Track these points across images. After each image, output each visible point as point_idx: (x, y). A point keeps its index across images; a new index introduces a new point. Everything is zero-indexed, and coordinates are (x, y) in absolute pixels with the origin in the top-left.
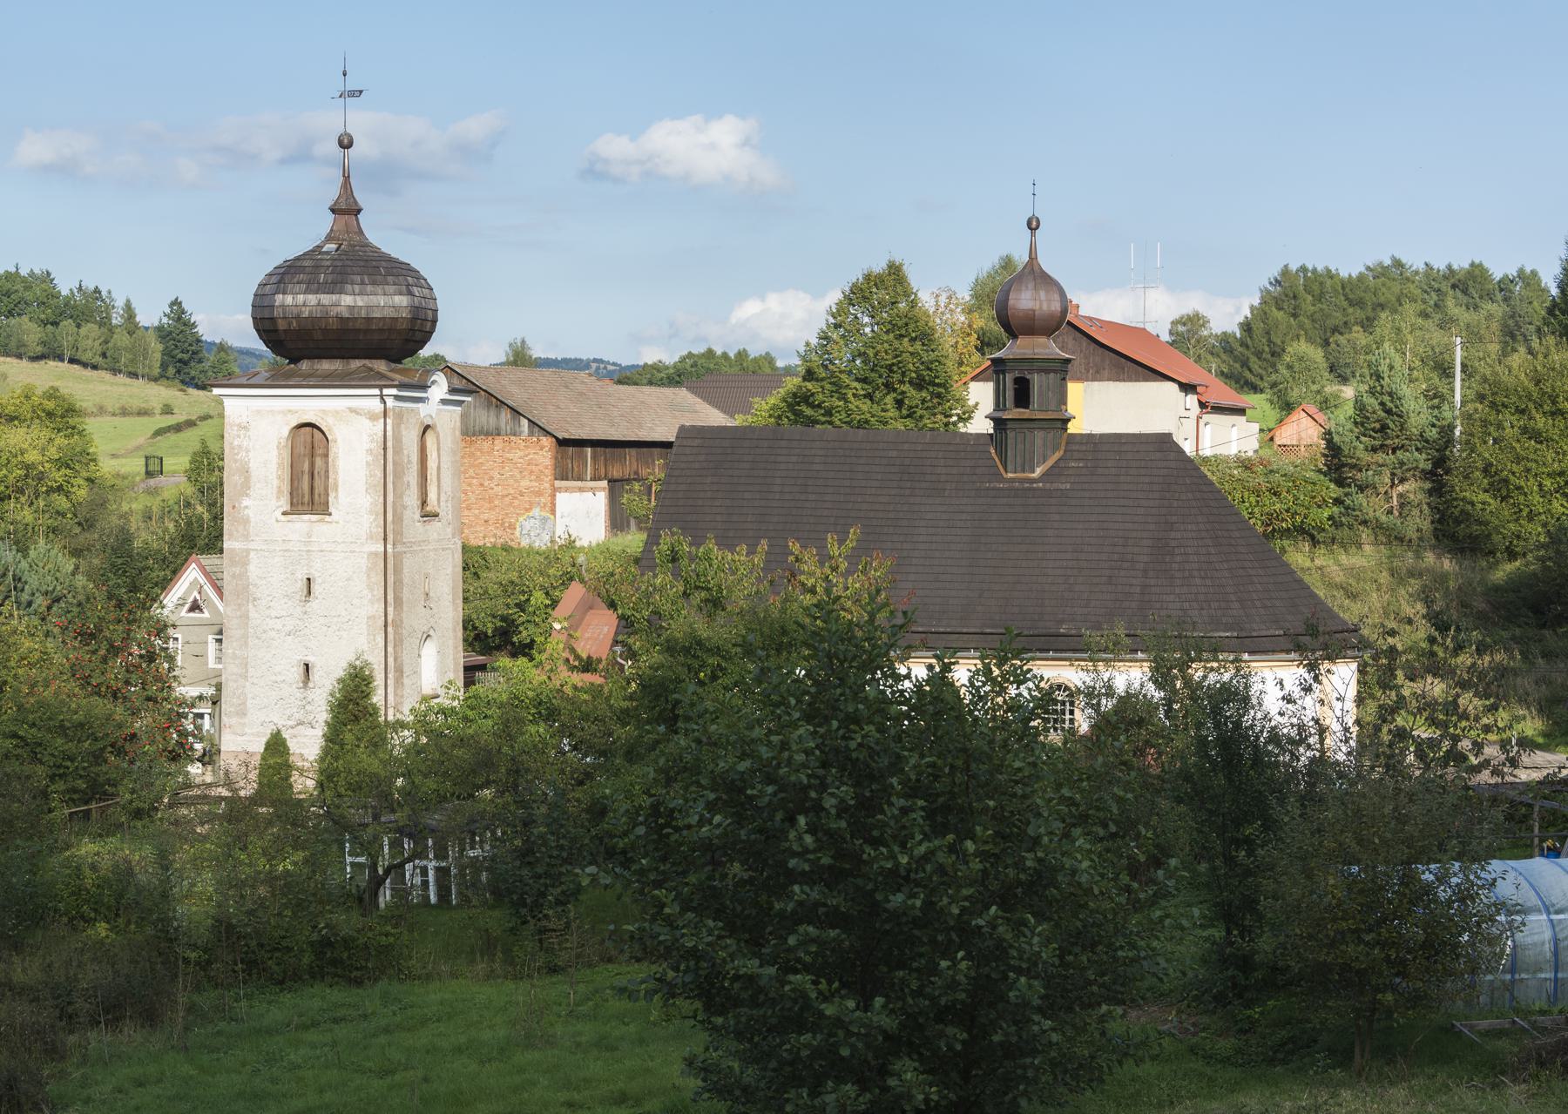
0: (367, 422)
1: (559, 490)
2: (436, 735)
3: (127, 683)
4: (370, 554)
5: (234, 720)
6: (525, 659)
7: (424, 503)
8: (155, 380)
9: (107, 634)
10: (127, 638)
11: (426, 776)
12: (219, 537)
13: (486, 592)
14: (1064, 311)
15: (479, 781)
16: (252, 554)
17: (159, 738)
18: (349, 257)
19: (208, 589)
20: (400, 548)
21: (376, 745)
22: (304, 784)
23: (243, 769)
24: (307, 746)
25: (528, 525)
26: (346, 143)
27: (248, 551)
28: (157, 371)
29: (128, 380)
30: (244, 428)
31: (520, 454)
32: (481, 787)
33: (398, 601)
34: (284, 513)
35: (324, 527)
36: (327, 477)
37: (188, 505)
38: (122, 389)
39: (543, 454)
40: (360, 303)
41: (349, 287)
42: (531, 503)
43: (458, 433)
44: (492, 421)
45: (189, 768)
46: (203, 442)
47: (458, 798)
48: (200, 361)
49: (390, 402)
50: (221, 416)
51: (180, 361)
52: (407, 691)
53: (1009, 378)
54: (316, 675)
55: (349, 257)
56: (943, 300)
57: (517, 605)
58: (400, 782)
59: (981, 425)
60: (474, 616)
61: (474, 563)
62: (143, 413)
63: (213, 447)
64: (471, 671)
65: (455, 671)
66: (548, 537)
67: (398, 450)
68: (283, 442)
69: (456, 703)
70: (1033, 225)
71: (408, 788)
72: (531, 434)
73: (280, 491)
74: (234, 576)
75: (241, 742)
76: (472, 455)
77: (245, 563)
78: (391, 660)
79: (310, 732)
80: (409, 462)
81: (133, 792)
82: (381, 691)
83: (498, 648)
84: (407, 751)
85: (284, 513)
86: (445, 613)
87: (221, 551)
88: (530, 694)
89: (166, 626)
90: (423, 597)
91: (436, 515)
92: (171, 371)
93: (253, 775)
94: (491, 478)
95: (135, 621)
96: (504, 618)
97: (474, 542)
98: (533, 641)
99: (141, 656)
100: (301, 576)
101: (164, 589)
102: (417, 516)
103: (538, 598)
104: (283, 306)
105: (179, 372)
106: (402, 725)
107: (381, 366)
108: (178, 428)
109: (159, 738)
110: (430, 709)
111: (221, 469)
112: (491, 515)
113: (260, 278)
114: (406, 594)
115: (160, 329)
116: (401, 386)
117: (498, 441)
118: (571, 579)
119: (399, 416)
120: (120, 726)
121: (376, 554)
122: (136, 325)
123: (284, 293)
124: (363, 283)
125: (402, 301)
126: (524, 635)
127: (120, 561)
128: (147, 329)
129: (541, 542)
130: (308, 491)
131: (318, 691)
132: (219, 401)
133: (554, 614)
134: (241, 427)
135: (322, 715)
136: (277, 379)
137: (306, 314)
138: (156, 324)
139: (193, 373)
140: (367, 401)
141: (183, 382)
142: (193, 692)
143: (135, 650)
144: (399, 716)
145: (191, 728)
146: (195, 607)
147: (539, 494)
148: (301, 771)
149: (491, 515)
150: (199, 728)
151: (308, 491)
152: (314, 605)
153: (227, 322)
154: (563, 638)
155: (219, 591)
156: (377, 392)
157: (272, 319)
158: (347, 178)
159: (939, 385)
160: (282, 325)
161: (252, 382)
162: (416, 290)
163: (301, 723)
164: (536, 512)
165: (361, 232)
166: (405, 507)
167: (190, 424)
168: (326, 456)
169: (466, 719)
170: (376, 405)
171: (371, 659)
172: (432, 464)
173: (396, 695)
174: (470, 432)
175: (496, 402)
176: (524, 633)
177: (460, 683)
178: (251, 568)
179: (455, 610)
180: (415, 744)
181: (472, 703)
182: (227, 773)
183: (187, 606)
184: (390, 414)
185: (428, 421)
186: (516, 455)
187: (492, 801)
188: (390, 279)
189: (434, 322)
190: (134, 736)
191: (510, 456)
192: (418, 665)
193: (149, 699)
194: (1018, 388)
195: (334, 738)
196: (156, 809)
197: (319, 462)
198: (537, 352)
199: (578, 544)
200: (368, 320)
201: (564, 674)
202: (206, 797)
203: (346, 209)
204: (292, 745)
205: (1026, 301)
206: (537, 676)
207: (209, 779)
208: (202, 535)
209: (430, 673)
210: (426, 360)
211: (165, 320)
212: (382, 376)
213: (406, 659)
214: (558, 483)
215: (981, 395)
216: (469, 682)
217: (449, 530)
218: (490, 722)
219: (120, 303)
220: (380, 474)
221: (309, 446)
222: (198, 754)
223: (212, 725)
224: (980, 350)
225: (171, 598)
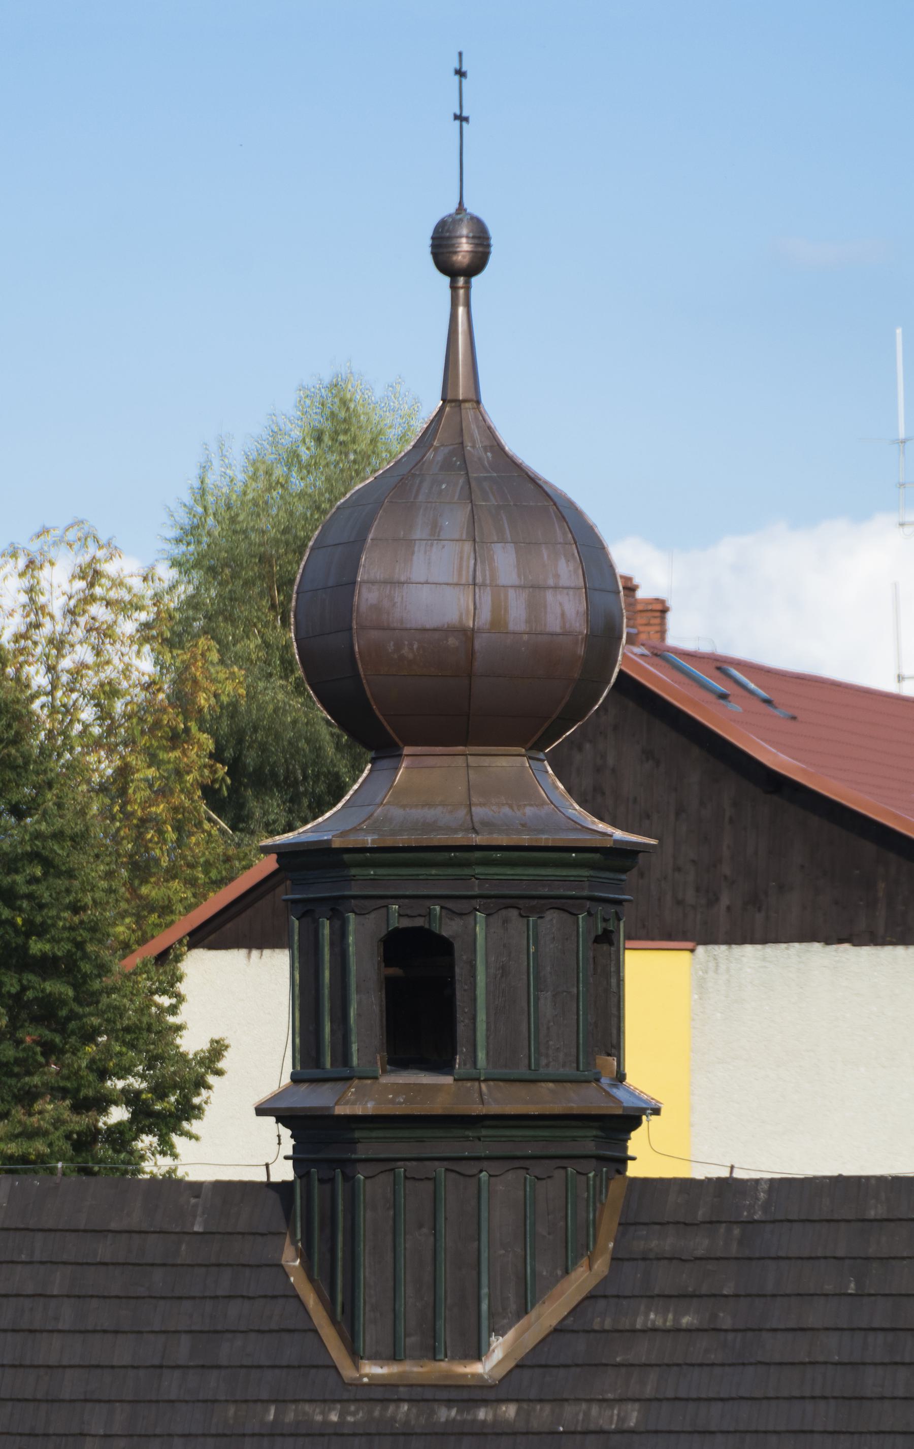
14: (604, 637)
53: (361, 936)
56: (59, 582)
59: (233, 1142)
70: (460, 254)
159: (47, 966)
194: (400, 980)
205: (435, 586)
215: (238, 1009)
224: (228, 803)
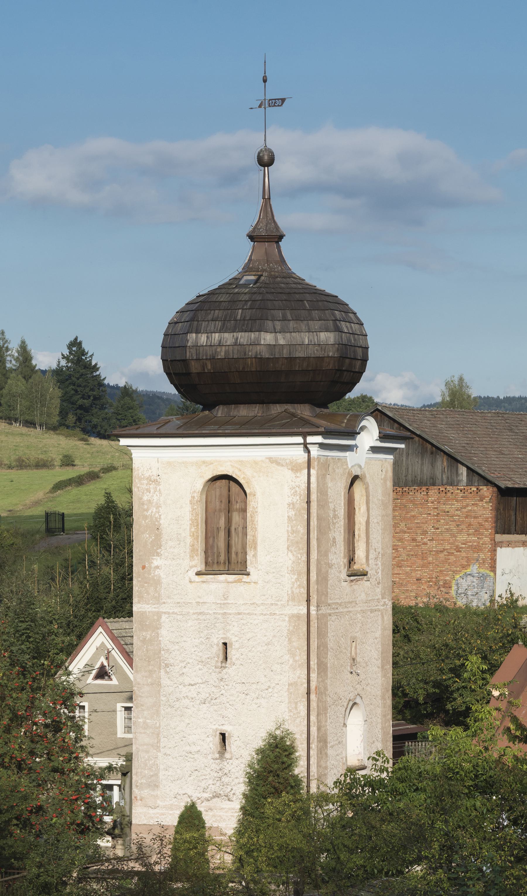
0: (288, 474)
1: (501, 544)
2: (363, 809)
3: (32, 753)
4: (292, 616)
5: (145, 793)
6: (459, 730)
7: (351, 561)
8: (54, 429)
9: (10, 702)
10: (32, 706)
11: (351, 851)
12: (128, 598)
13: (417, 656)
15: (409, 857)
16: (164, 617)
17: (66, 810)
18: (269, 289)
19: (116, 655)
20: (324, 610)
21: (299, 819)
22: (221, 859)
23: (158, 843)
24: (224, 818)
25: (464, 584)
26: (266, 160)
27: (159, 615)
28: (55, 419)
29: (25, 430)
30: (155, 481)
31: (457, 505)
32: (412, 863)
33: (322, 667)
34: (198, 574)
35: (241, 588)
36: (245, 534)
37: (93, 564)
38: (18, 439)
39: (482, 505)
40: (282, 342)
41: (270, 323)
42: (468, 560)
43: (390, 484)
44: (427, 469)
45: (99, 842)
46: (108, 496)
47: (387, 874)
48: (102, 408)
49: (315, 451)
50: (129, 467)
51: (81, 407)
52: (331, 762)
54: (232, 744)
55: (269, 289)
57: (452, 670)
58: (323, 857)
60: (404, 682)
61: (406, 625)
62: (42, 465)
63: (120, 501)
64: (399, 740)
65: (384, 741)
66: (487, 597)
67: (323, 504)
68: (197, 496)
69: (384, 775)
71: (333, 863)
72: (470, 483)
73: (193, 550)
74: (144, 641)
75: (153, 813)
76: (404, 507)
77: (156, 627)
78: (314, 730)
79: (226, 805)
80: (335, 516)
81: (40, 865)
82: (303, 763)
83: (430, 716)
84: (332, 826)
85: (198, 574)
86: (375, 679)
87: (130, 614)
88: (467, 766)
89: (72, 695)
90: (349, 662)
91: (365, 574)
92: (71, 418)
93: (167, 850)
94: (425, 533)
95: (39, 688)
96: (437, 684)
97: (405, 602)
98: (468, 709)
99: (46, 726)
100: (217, 640)
101: (69, 654)
102: (343, 575)
103: (474, 662)
104: (196, 346)
105: (79, 419)
106: (324, 798)
107: (304, 411)
108: (79, 481)
109: (66, 810)
110: (355, 780)
111: (129, 526)
112: (425, 574)
113: (170, 314)
114: (331, 660)
115: (58, 372)
116: (326, 434)
117: (433, 491)
118: (513, 642)
120: (25, 798)
121: (298, 616)
122: (33, 369)
123: (197, 332)
124: (284, 319)
125: (327, 337)
126: (458, 702)
127: (24, 625)
128: (44, 372)
129: (480, 601)
130: (224, 550)
131: (236, 762)
132: (126, 452)
133: (493, 680)
134: (150, 480)
135: (239, 787)
136: (193, 426)
137: (222, 355)
138: (54, 366)
139: (95, 421)
140: (288, 449)
141: (85, 431)
142: (102, 762)
143: (40, 719)
144: (323, 788)
145: (99, 800)
146: (102, 674)
147: (478, 549)
148: (219, 846)
149: (425, 574)
150: (108, 800)
151: (224, 550)
152: (231, 670)
153: (135, 363)
154: (502, 705)
155: (128, 656)
156: (299, 439)
157: (185, 362)
158: (267, 200)
160: (195, 368)
161: (162, 431)
162: (344, 326)
163: (217, 796)
164: (474, 569)
165: (283, 261)
166: (330, 566)
167: (93, 476)
169: (394, 792)
170: (299, 454)
171: (292, 728)
172: (360, 518)
173: (319, 766)
174: (402, 481)
175: (428, 448)
176: (459, 700)
177: (389, 754)
178: (163, 632)
179: (384, 676)
180: (341, 818)
181: (402, 775)
182: (140, 847)
183: (94, 672)
184: (314, 464)
185: (357, 472)
186: (453, 507)
187: (423, 877)
188: (315, 314)
189: (364, 360)
190: (40, 808)
191: (447, 508)
192: (344, 735)
193: (55, 770)
195: (253, 808)
196: (65, 884)
197: (236, 518)
198: (476, 390)
199: (520, 603)
200: (291, 360)
201: (502, 742)
202: (117, 871)
203: (267, 236)
204: (209, 819)
206: (474, 746)
207: (120, 852)
208: (111, 597)
209: (358, 739)
210: (352, 402)
211: (63, 363)
212: (305, 422)
213: (330, 728)
214: (499, 537)
216: (398, 753)
217: (379, 590)
218: (423, 796)
219: (14, 346)
220: (303, 530)
221: (225, 500)
222: (107, 827)
223: (122, 797)
225: (77, 664)
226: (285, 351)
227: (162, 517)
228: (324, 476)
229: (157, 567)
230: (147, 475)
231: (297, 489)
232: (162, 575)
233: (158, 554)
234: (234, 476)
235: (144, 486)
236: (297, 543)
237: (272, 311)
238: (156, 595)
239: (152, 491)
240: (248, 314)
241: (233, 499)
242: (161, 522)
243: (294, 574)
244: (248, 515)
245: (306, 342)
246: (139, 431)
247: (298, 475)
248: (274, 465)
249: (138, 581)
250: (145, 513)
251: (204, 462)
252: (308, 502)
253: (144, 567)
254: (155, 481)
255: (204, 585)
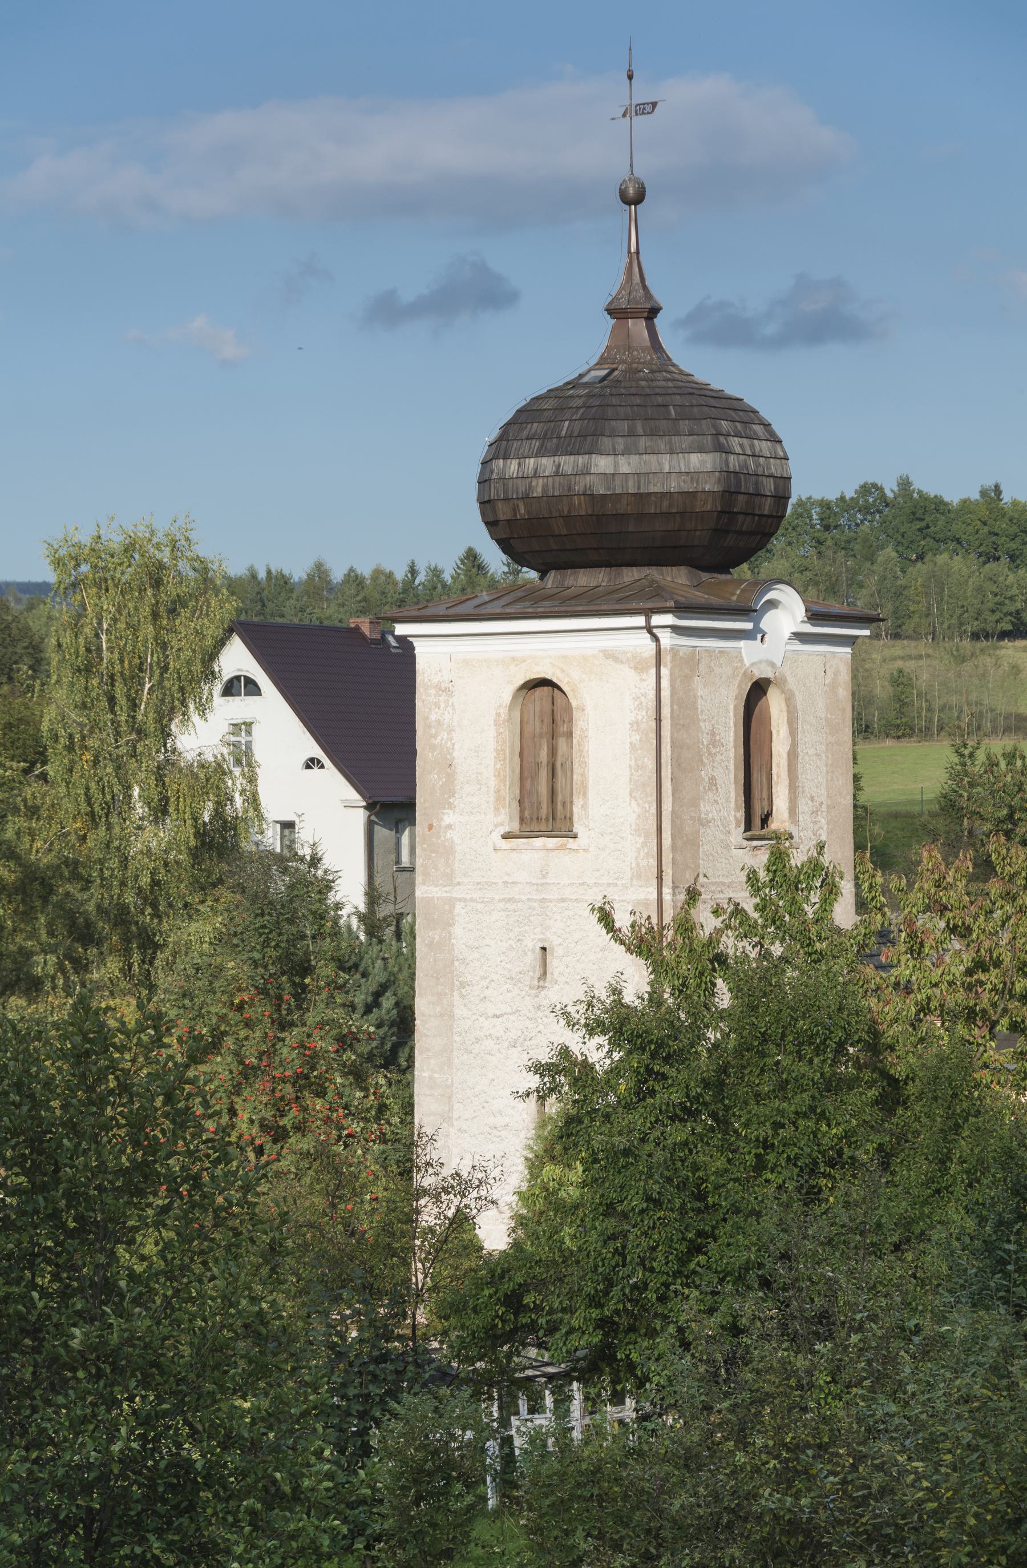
16: (458, 907)
27: (451, 902)
30: (445, 690)
34: (506, 836)
40: (624, 469)
49: (667, 639)
68: (504, 712)
85: (506, 836)
100: (532, 944)
116: (681, 609)
119: (690, 663)
124: (632, 434)
137: (538, 492)
168: (570, 735)
178: (457, 930)
184: (666, 659)
220: (652, 765)
221: (547, 720)
226: (631, 483)
227: (456, 747)
228: (688, 679)
229: (449, 827)
230: (435, 681)
231: (643, 699)
232: (457, 841)
233: (451, 806)
234: (555, 680)
235: (432, 699)
236: (644, 785)
237: (613, 423)
238: (448, 871)
239: (442, 705)
240: (577, 426)
241: (558, 718)
242: (455, 754)
243: (640, 836)
244: (575, 741)
245: (667, 469)
246: (424, 612)
247: (644, 676)
248: (610, 661)
249: (424, 849)
250: (433, 740)
251: (513, 659)
252: (659, 720)
253: (431, 827)
254: (447, 690)
255: (514, 854)
